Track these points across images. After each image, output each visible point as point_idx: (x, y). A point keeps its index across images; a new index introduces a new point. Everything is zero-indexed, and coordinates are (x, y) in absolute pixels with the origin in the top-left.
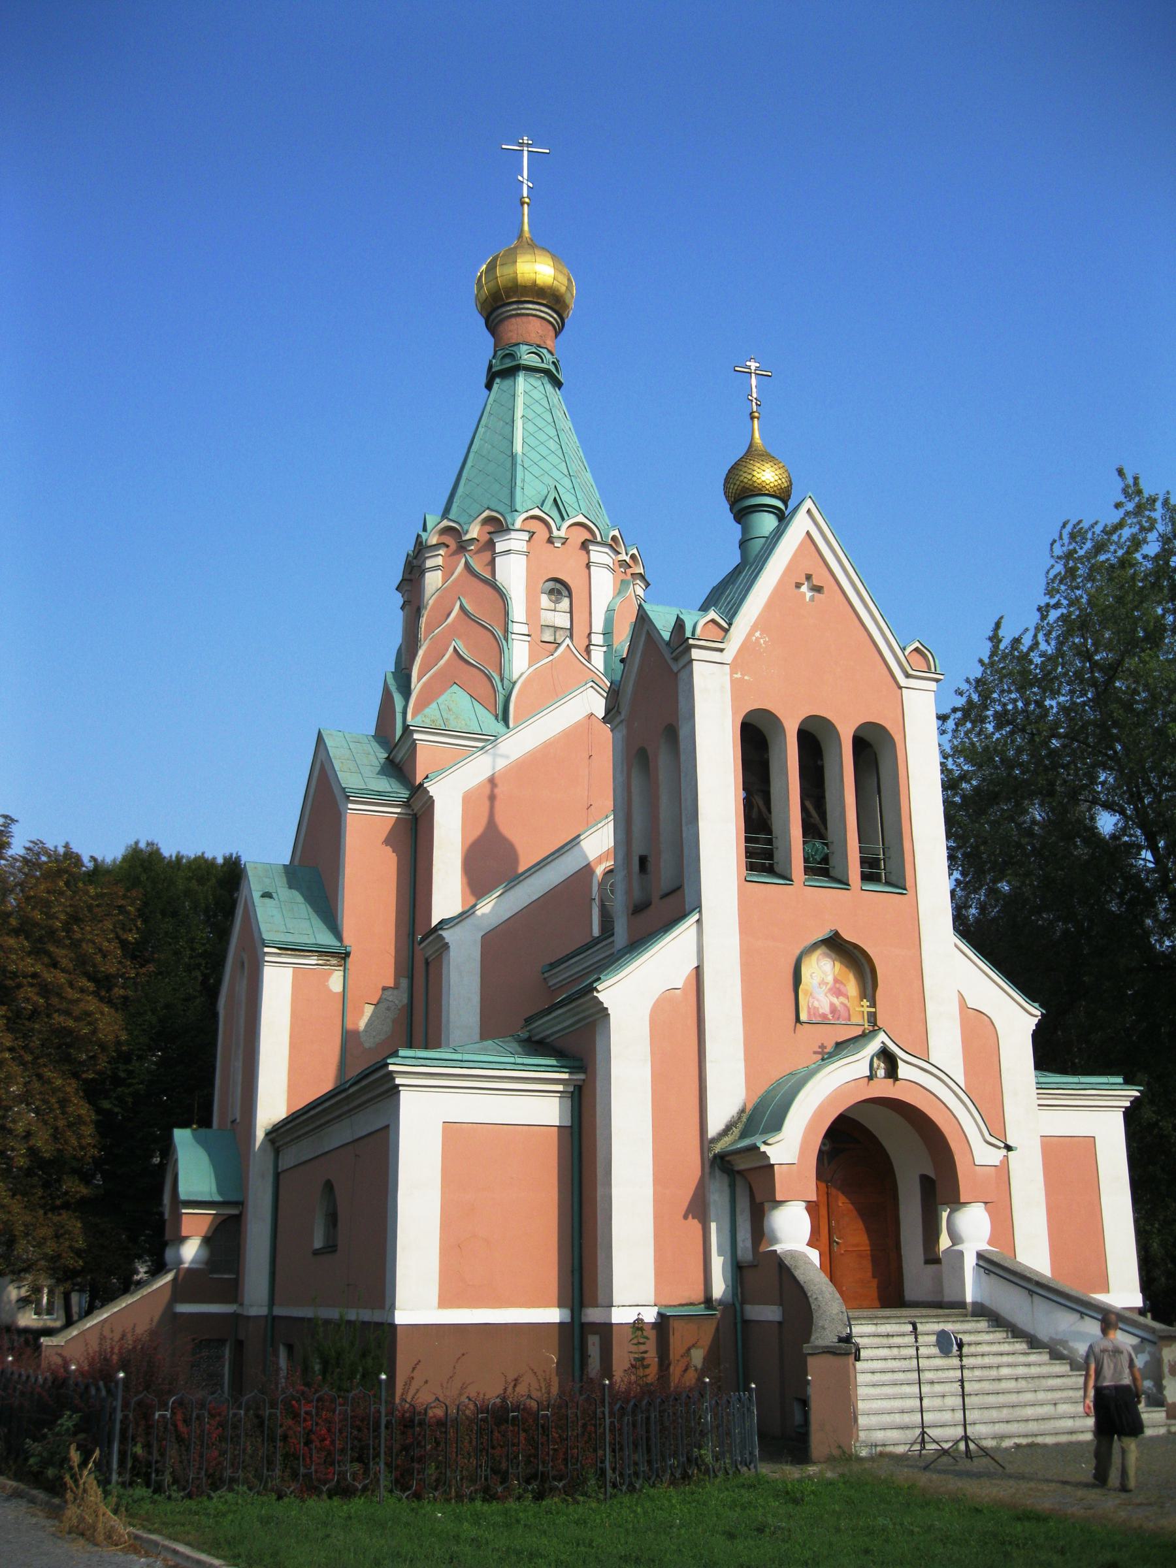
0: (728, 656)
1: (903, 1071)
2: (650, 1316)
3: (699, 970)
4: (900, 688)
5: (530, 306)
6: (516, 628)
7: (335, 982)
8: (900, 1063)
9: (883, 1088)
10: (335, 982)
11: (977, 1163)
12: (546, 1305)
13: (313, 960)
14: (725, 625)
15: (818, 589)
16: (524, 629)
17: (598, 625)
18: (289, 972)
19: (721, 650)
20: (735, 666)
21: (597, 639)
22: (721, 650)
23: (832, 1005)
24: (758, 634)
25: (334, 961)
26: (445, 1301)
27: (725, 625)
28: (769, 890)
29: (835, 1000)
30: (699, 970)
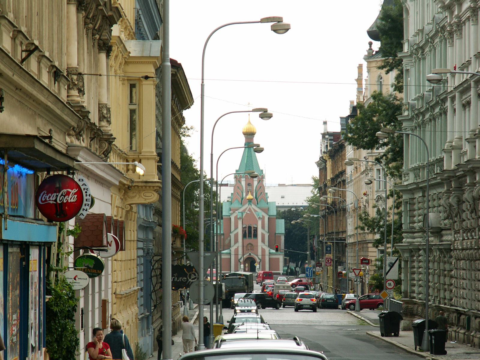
9: (250, 256)
17: (254, 189)
21: (254, 191)
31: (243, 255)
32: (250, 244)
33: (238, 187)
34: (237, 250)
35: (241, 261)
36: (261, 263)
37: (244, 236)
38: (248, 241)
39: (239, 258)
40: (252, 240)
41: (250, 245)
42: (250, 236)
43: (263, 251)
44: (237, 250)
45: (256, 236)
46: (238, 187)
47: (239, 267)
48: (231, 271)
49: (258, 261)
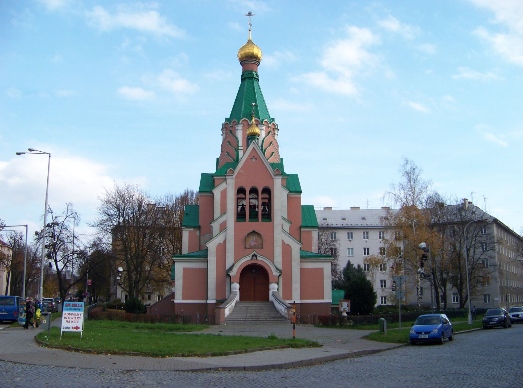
0: (234, 177)
1: (258, 258)
2: (214, 302)
3: (225, 240)
4: (273, 178)
5: (249, 61)
6: (240, 148)
7: (198, 233)
8: (258, 257)
9: (253, 262)
10: (198, 233)
11: (274, 275)
12: (204, 300)
13: (192, 229)
14: (233, 170)
15: (256, 159)
16: (242, 148)
18: (188, 232)
19: (233, 176)
20: (235, 178)
22: (233, 176)
23: (255, 244)
24: (241, 171)
25: (197, 229)
26: (183, 299)
27: (233, 170)
28: (242, 224)
29: (255, 243)
30: (225, 240)
31: (236, 260)
32: (254, 233)
33: (229, 142)
34: (222, 248)
35: (231, 274)
36: (281, 279)
37: (240, 216)
38: (249, 225)
39: (228, 267)
40: (259, 225)
41: (254, 238)
42: (254, 216)
43: (287, 250)
44: (222, 248)
45: (268, 216)
46: (229, 142)
47: (228, 289)
48: (207, 300)
49: (276, 274)
